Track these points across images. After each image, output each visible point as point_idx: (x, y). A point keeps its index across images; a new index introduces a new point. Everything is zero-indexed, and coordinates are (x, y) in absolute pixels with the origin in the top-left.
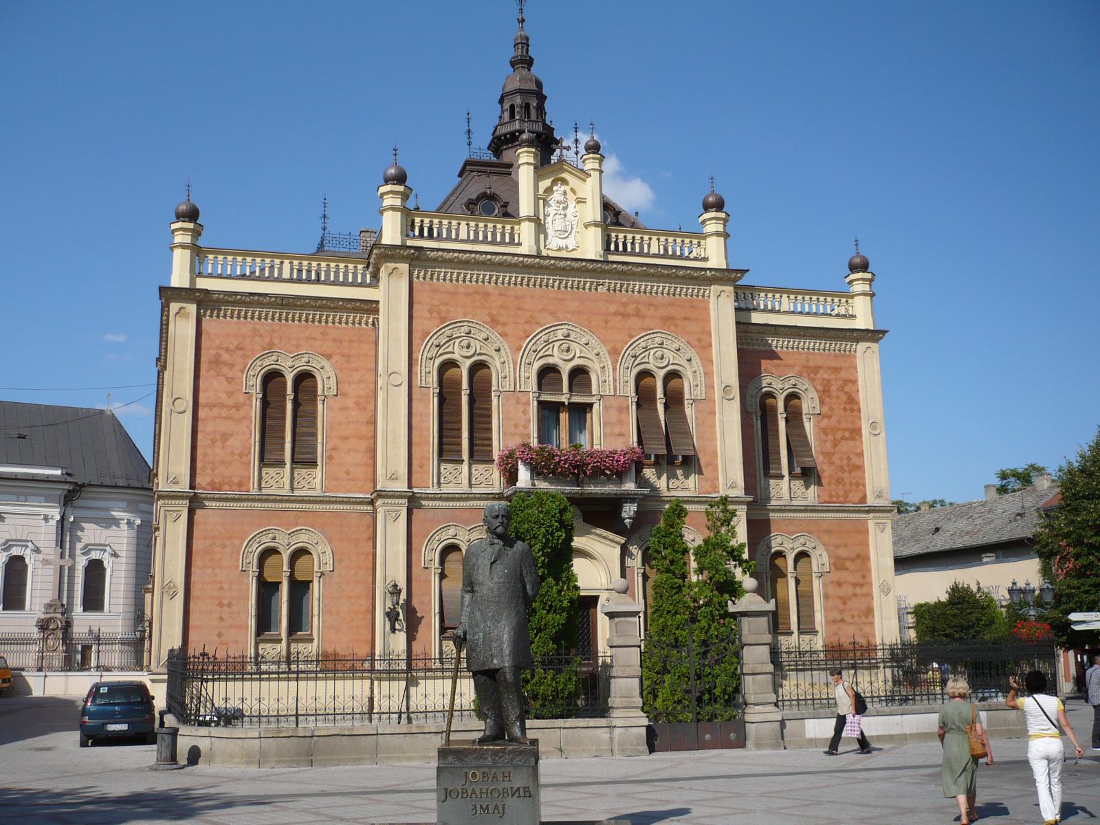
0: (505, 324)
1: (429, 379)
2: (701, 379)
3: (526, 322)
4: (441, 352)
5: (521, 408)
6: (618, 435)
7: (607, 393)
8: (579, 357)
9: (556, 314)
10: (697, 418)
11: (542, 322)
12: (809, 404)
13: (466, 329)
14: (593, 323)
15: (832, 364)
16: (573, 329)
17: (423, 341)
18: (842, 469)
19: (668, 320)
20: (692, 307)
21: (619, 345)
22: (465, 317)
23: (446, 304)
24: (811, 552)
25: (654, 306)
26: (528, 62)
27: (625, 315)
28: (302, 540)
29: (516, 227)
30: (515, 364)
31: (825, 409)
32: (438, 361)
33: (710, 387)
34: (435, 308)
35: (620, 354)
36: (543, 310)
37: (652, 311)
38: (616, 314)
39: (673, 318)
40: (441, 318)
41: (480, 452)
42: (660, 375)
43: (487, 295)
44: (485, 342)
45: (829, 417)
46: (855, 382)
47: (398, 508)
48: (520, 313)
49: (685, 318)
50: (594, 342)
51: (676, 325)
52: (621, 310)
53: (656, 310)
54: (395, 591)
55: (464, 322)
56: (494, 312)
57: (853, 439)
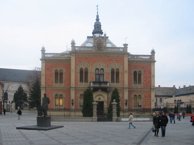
1: (78, 71)
12: (142, 73)
15: (147, 66)
18: (147, 82)
19: (117, 61)
24: (141, 96)
26: (99, 20)
27: (110, 60)
28: (61, 93)
31: (145, 73)
33: (124, 71)
41: (86, 81)
42: (115, 69)
45: (145, 74)
46: (151, 69)
54: (73, 100)
57: (149, 78)
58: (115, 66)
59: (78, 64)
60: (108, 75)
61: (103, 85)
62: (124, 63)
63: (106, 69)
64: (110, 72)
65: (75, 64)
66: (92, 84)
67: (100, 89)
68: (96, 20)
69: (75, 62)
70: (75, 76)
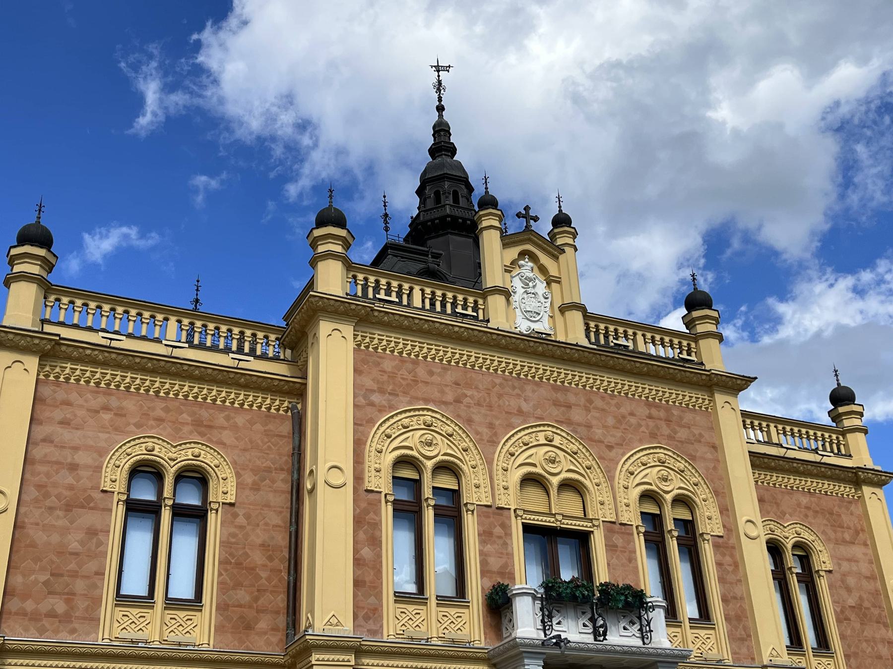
1: (380, 482)
4: (395, 444)
12: (823, 560)
16: (558, 431)
29: (481, 301)
32: (389, 458)
64: (632, 517)
68: (433, 152)
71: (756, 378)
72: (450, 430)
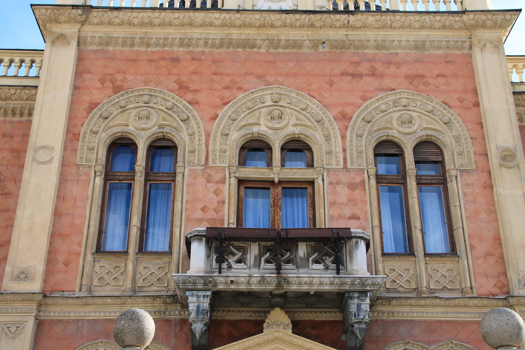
0: (197, 91)
2: (469, 148)
3: (225, 88)
5: (212, 187)
6: (350, 218)
7: (334, 166)
8: (296, 125)
9: (264, 77)
10: (465, 194)
11: (245, 87)
13: (146, 98)
14: (314, 87)
17: (89, 113)
19: (414, 79)
20: (447, 62)
21: (348, 110)
22: (146, 85)
23: (124, 72)
25: (396, 64)
30: (208, 135)
34: (108, 78)
35: (351, 119)
36: (246, 74)
37: (392, 70)
38: (344, 74)
39: (422, 76)
40: (114, 87)
43: (176, 60)
44: (169, 112)
47: (19, 319)
48: (217, 78)
49: (438, 76)
50: (314, 106)
51: (426, 84)
52: (351, 70)
53: (399, 68)
55: (143, 90)
56: (184, 79)
58: (406, 115)
59: (93, 106)
60: (352, 186)
61: (312, 276)
62: (475, 92)
63: (327, 138)
65: (73, 103)
66: (199, 250)
67: (278, 316)
69: (76, 88)
70: (60, 197)
71: (520, 10)
72: (169, 104)
